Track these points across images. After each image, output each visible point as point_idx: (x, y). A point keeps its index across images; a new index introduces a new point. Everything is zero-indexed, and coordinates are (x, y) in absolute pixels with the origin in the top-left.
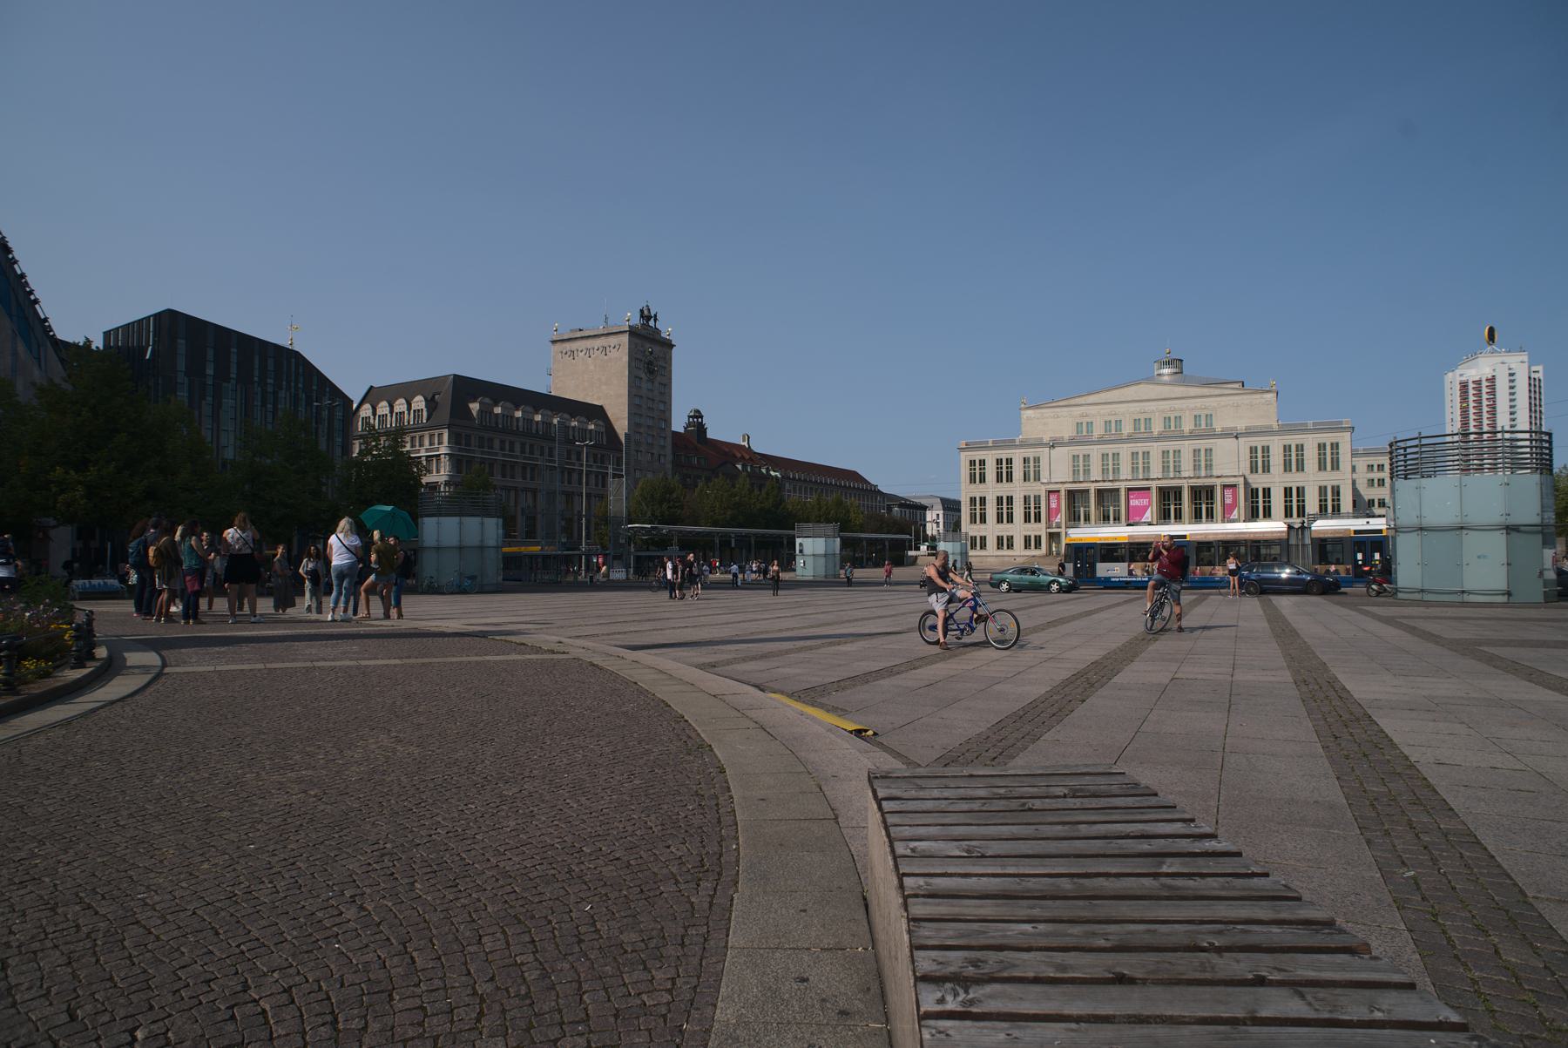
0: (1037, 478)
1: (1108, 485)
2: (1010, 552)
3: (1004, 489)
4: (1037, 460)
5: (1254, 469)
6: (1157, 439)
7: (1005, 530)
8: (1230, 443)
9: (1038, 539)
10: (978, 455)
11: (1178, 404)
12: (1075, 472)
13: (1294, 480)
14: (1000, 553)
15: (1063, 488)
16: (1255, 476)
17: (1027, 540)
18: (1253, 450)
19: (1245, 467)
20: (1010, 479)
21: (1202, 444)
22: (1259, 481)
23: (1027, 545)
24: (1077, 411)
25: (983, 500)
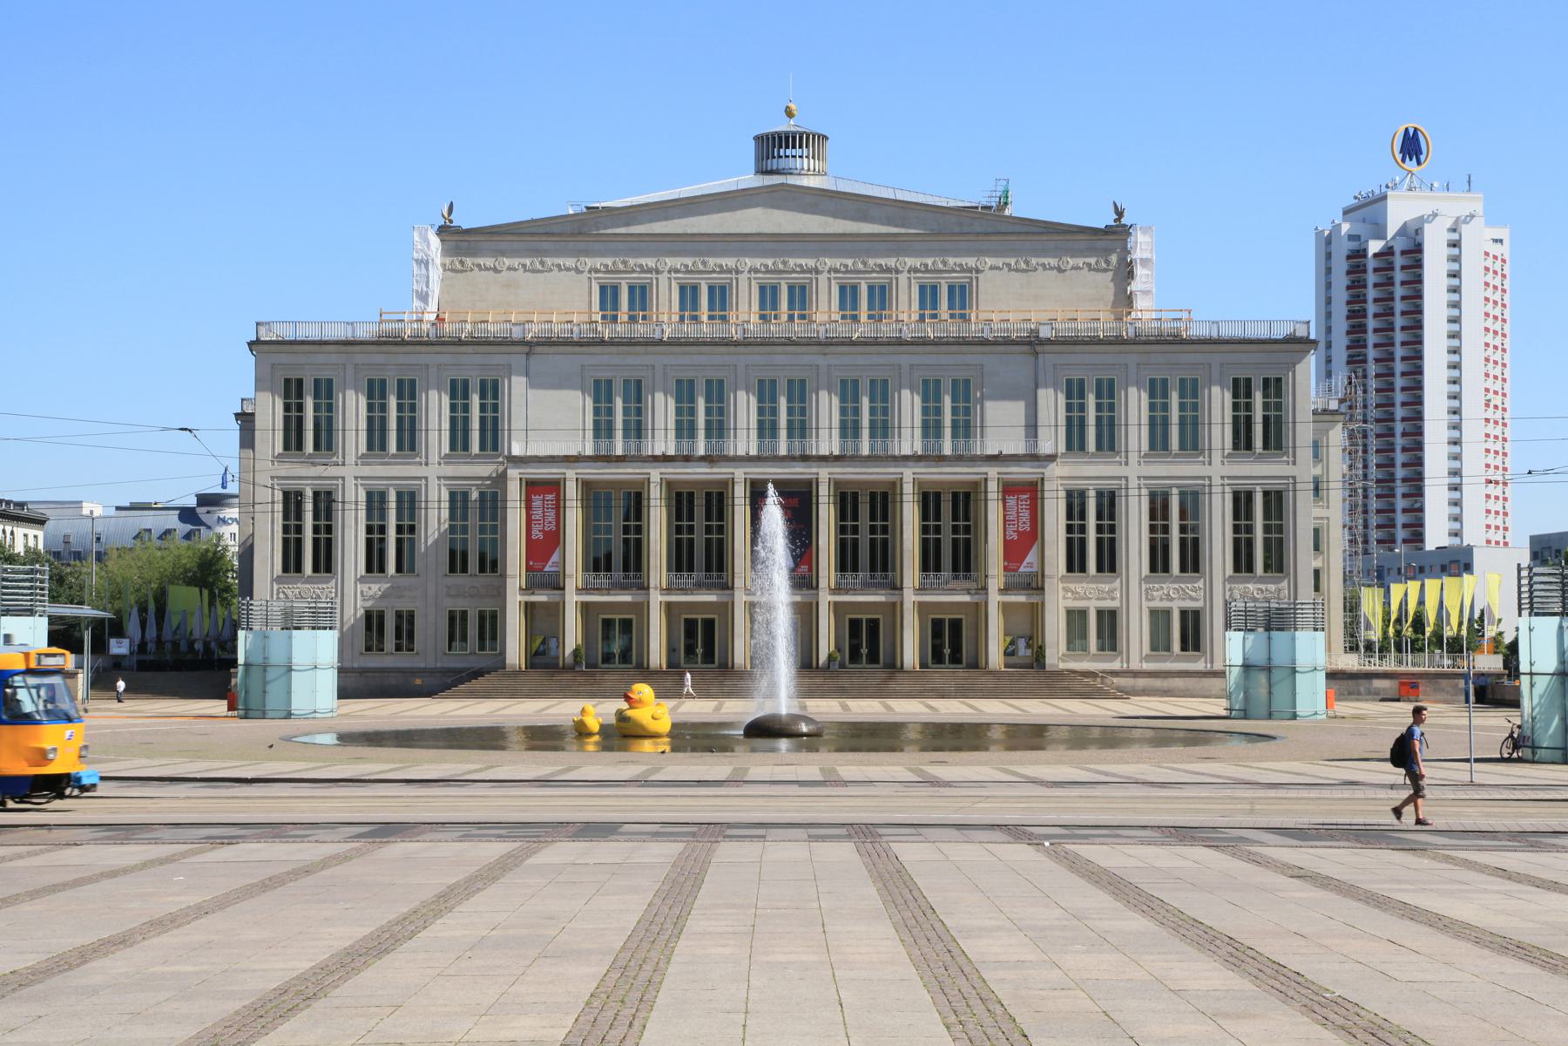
5: (1075, 442)
12: (603, 429)
19: (1051, 440)
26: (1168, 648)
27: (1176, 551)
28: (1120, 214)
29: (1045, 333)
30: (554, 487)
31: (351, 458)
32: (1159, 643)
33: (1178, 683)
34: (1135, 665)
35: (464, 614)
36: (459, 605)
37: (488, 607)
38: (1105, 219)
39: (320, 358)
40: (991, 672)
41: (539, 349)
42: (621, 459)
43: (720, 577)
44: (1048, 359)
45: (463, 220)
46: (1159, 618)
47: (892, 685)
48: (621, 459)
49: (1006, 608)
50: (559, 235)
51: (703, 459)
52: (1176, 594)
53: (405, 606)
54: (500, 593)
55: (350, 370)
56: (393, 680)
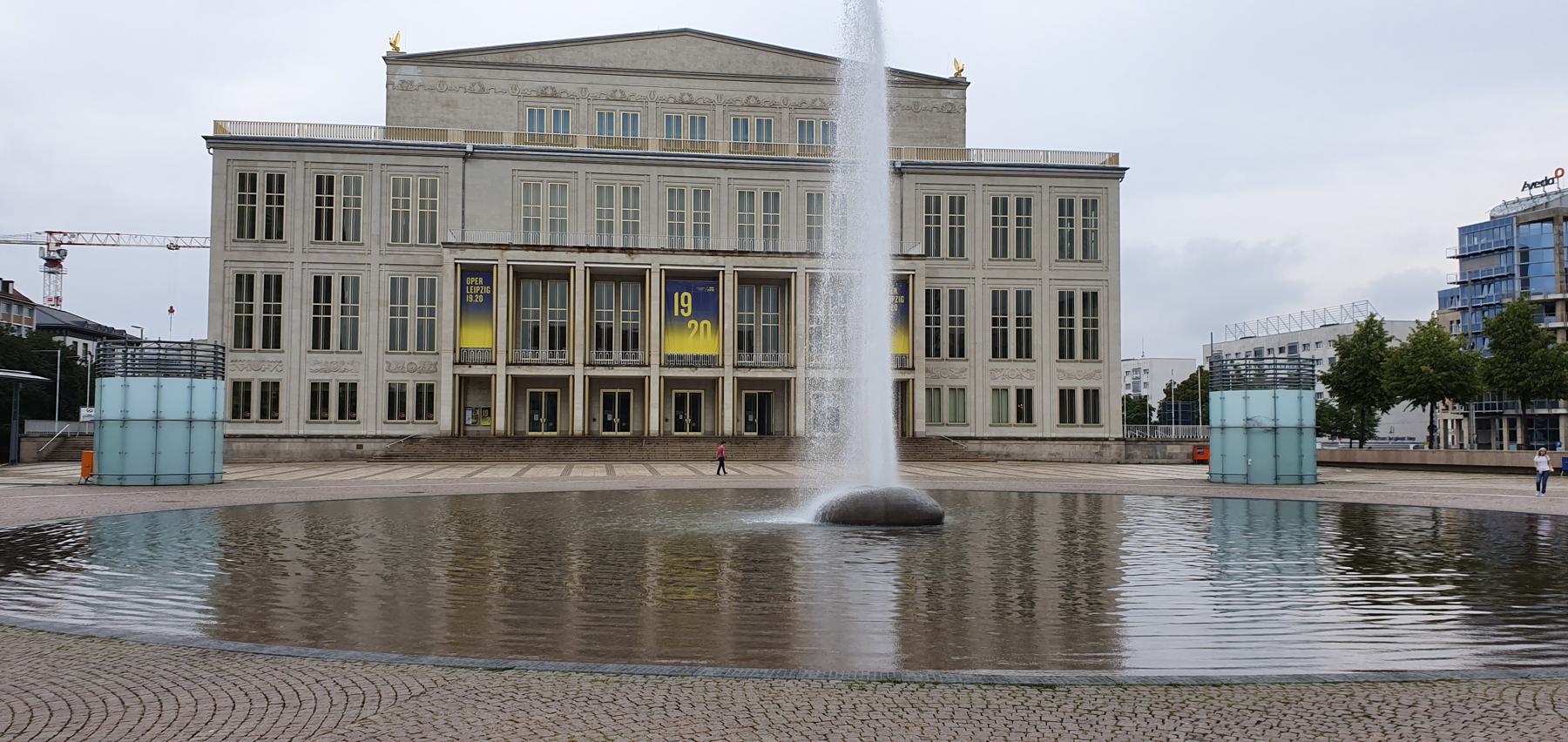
0: (428, 232)
1: (619, 261)
2: (347, 429)
4: (427, 189)
5: (932, 250)
6: (726, 164)
7: (333, 368)
9: (426, 396)
11: (765, 92)
13: (1012, 275)
14: (318, 429)
15: (502, 262)
16: (932, 262)
18: (932, 204)
22: (948, 274)
23: (395, 405)
24: (532, 81)
25: (274, 286)
27: (1012, 340)
30: (485, 273)
31: (298, 248)
33: (1015, 448)
36: (397, 378)
37: (425, 379)
38: (948, 73)
42: (550, 248)
43: (636, 356)
45: (408, 48)
50: (494, 64)
51: (622, 250)
52: (1013, 374)
53: (347, 378)
54: (435, 369)
55: (300, 166)
56: (336, 445)
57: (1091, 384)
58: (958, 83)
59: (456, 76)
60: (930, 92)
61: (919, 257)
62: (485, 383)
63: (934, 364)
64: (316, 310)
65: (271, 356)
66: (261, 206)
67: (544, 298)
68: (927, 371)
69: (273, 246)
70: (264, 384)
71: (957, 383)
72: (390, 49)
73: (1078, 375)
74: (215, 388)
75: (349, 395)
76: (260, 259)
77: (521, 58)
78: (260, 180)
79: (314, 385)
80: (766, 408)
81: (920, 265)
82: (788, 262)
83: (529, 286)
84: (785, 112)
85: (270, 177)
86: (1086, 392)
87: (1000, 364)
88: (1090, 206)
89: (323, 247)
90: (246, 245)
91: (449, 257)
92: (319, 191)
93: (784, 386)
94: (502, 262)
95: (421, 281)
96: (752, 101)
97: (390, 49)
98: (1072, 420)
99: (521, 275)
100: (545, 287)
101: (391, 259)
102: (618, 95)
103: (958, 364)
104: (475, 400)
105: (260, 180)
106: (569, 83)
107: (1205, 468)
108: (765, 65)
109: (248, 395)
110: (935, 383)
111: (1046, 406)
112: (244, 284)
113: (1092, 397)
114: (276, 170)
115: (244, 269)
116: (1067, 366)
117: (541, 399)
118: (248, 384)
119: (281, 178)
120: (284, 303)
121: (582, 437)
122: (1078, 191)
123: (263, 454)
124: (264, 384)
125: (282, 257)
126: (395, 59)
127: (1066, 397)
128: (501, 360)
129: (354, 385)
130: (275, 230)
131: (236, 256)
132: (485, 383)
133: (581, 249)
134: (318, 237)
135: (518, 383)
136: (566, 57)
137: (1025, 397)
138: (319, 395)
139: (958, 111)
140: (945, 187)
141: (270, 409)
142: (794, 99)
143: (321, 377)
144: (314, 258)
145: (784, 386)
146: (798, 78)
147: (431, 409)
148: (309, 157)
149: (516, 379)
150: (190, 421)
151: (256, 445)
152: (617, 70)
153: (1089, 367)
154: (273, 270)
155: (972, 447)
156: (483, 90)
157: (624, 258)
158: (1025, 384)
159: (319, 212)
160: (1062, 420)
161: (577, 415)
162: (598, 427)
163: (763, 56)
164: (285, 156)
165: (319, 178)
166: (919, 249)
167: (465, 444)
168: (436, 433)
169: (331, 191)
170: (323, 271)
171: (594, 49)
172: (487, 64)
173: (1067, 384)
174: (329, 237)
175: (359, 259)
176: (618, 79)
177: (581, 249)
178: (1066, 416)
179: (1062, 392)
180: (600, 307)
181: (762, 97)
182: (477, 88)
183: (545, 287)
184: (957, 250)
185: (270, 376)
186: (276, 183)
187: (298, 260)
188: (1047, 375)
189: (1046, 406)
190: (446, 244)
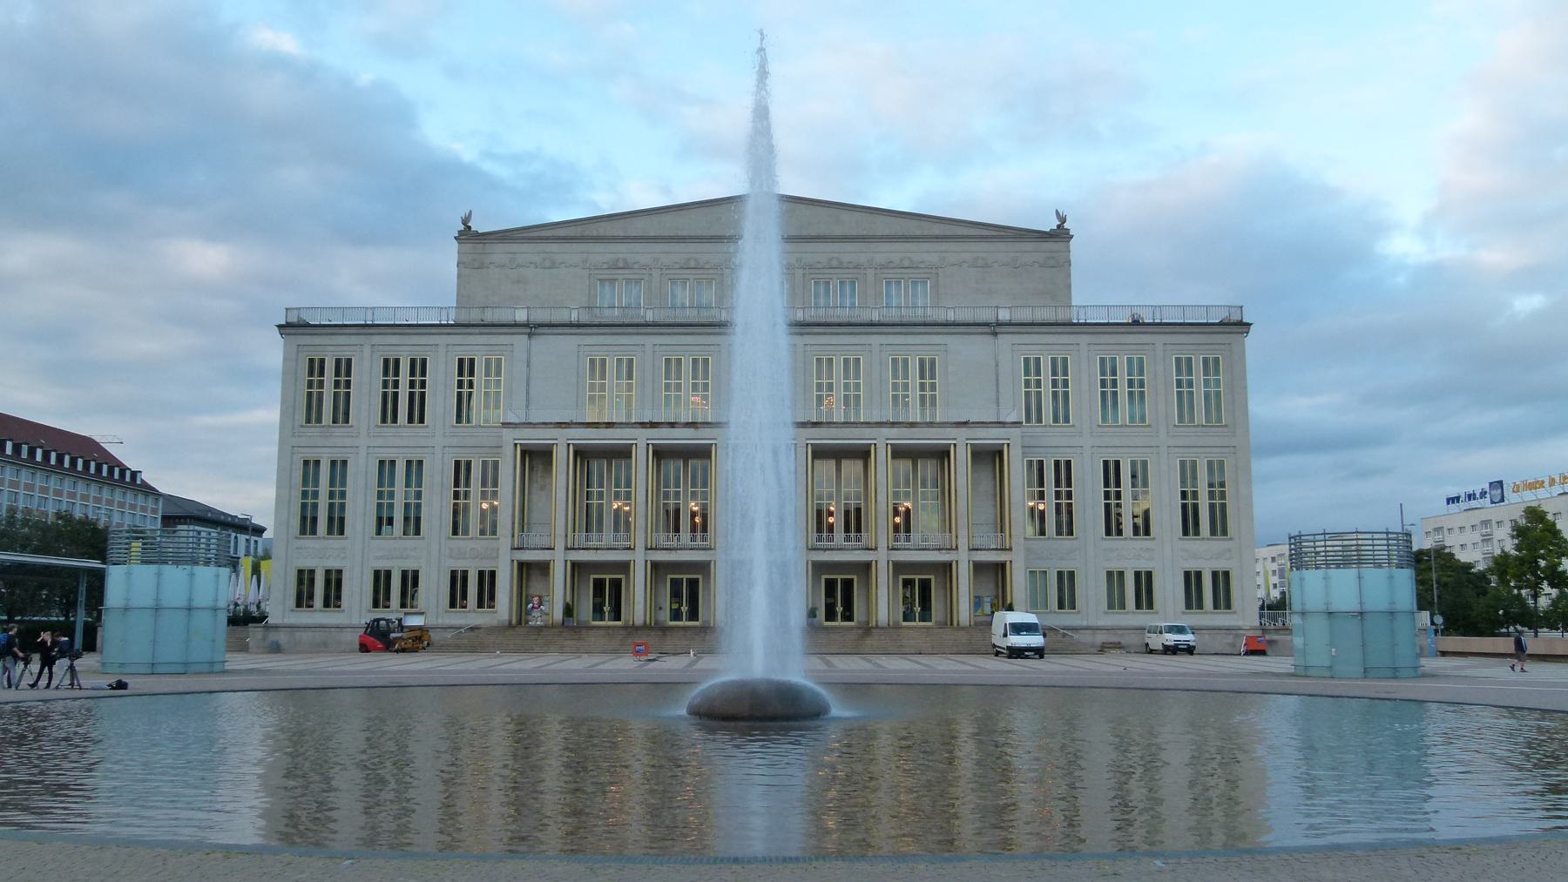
3: (401, 441)
5: (1033, 412)
8: (974, 348)
9: (488, 580)
10: (330, 350)
15: (562, 444)
16: (1034, 430)
17: (458, 582)
20: (417, 413)
21: (916, 347)
22: (1054, 442)
23: (457, 593)
24: (601, 254)
26: (1123, 606)
28: (1063, 220)
29: (1004, 315)
32: (1115, 602)
34: (1092, 623)
35: (465, 573)
36: (460, 565)
37: (487, 566)
38: (1051, 224)
39: (341, 340)
40: (963, 628)
41: (541, 330)
42: (610, 425)
44: (1005, 340)
45: (478, 226)
46: (1115, 579)
47: (868, 641)
48: (610, 425)
49: (979, 568)
53: (410, 565)
55: (367, 350)
57: (1221, 566)
58: (1060, 234)
59: (526, 252)
60: (1029, 246)
61: (1017, 424)
62: (544, 568)
63: (1040, 544)
64: (380, 495)
65: (335, 542)
66: (328, 391)
67: (609, 478)
68: (1028, 550)
69: (339, 430)
70: (328, 572)
71: (1066, 567)
72: (462, 227)
73: (1205, 554)
74: (217, 576)
75: (334, 582)
76: (326, 443)
77: (593, 230)
78: (326, 366)
79: (377, 573)
80: (686, 589)
81: (1015, 432)
82: (867, 432)
83: (672, 466)
84: (870, 273)
85: (338, 362)
86: (1215, 574)
87: (1114, 542)
88: (1211, 366)
89: (389, 430)
90: (313, 430)
91: (509, 436)
92: (386, 373)
93: (704, 567)
94: (562, 444)
95: (485, 463)
96: (835, 263)
97: (462, 227)
98: (1200, 606)
99: (583, 454)
100: (610, 465)
101: (454, 441)
102: (692, 264)
103: (1066, 543)
104: (536, 587)
105: (326, 366)
106: (642, 254)
107: (1290, 660)
108: (848, 225)
109: (312, 581)
110: (1039, 566)
111: (1169, 590)
112: (310, 467)
113: (1222, 580)
114: (344, 355)
115: (311, 455)
116: (1192, 544)
117: (606, 588)
118: (312, 572)
119: (349, 361)
120: (349, 490)
121: (645, 627)
122: (1197, 349)
123: (325, 644)
124: (328, 572)
125: (348, 442)
126: (467, 235)
127: (1192, 580)
128: (560, 546)
129: (340, 572)
130: (342, 414)
131: (303, 441)
132: (544, 568)
133: (643, 425)
134: (384, 420)
135: (578, 568)
136: (638, 227)
137: (1145, 583)
138: (381, 580)
139: (1063, 264)
140: (1045, 348)
141: (333, 597)
142: (880, 259)
143: (383, 565)
144: (379, 442)
145: (704, 567)
146: (882, 237)
147: (492, 597)
148: (377, 339)
149: (575, 565)
150: (189, 609)
151: (319, 636)
152: (691, 238)
153: (1218, 544)
154: (339, 457)
155: (1085, 637)
156: (553, 266)
157: (689, 432)
158: (1143, 566)
159: (385, 395)
160: (1189, 606)
161: (638, 601)
162: (665, 617)
163: (845, 216)
164: (354, 340)
165: (386, 361)
166: (1017, 414)
167: (522, 630)
168: (495, 623)
169: (397, 374)
170: (387, 455)
171: (667, 218)
172: (559, 238)
173: (1192, 566)
174: (395, 420)
175: (423, 442)
176: (691, 247)
177: (643, 425)
178: (1193, 598)
179: (1187, 574)
180: (666, 486)
181: (846, 258)
182: (547, 264)
183: (610, 465)
184: (1062, 416)
185: (334, 564)
186: (344, 367)
187: (365, 441)
188: (1169, 556)
189: (1169, 590)
190: (506, 425)
